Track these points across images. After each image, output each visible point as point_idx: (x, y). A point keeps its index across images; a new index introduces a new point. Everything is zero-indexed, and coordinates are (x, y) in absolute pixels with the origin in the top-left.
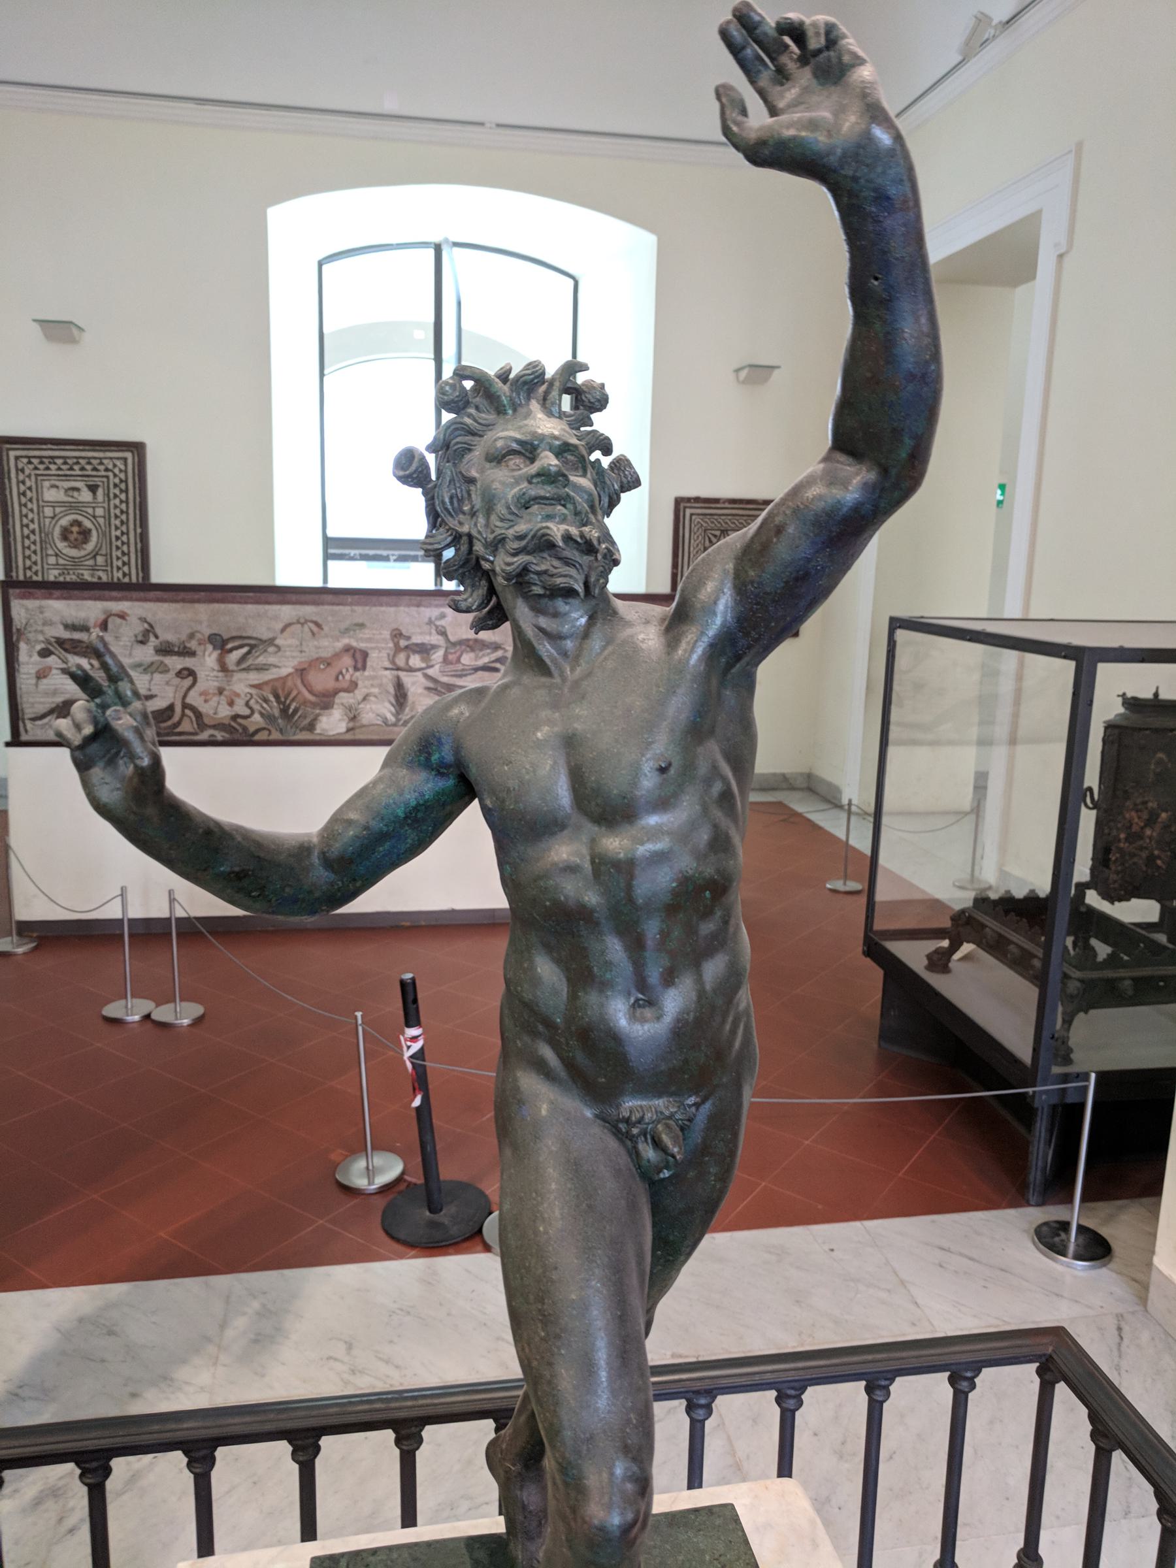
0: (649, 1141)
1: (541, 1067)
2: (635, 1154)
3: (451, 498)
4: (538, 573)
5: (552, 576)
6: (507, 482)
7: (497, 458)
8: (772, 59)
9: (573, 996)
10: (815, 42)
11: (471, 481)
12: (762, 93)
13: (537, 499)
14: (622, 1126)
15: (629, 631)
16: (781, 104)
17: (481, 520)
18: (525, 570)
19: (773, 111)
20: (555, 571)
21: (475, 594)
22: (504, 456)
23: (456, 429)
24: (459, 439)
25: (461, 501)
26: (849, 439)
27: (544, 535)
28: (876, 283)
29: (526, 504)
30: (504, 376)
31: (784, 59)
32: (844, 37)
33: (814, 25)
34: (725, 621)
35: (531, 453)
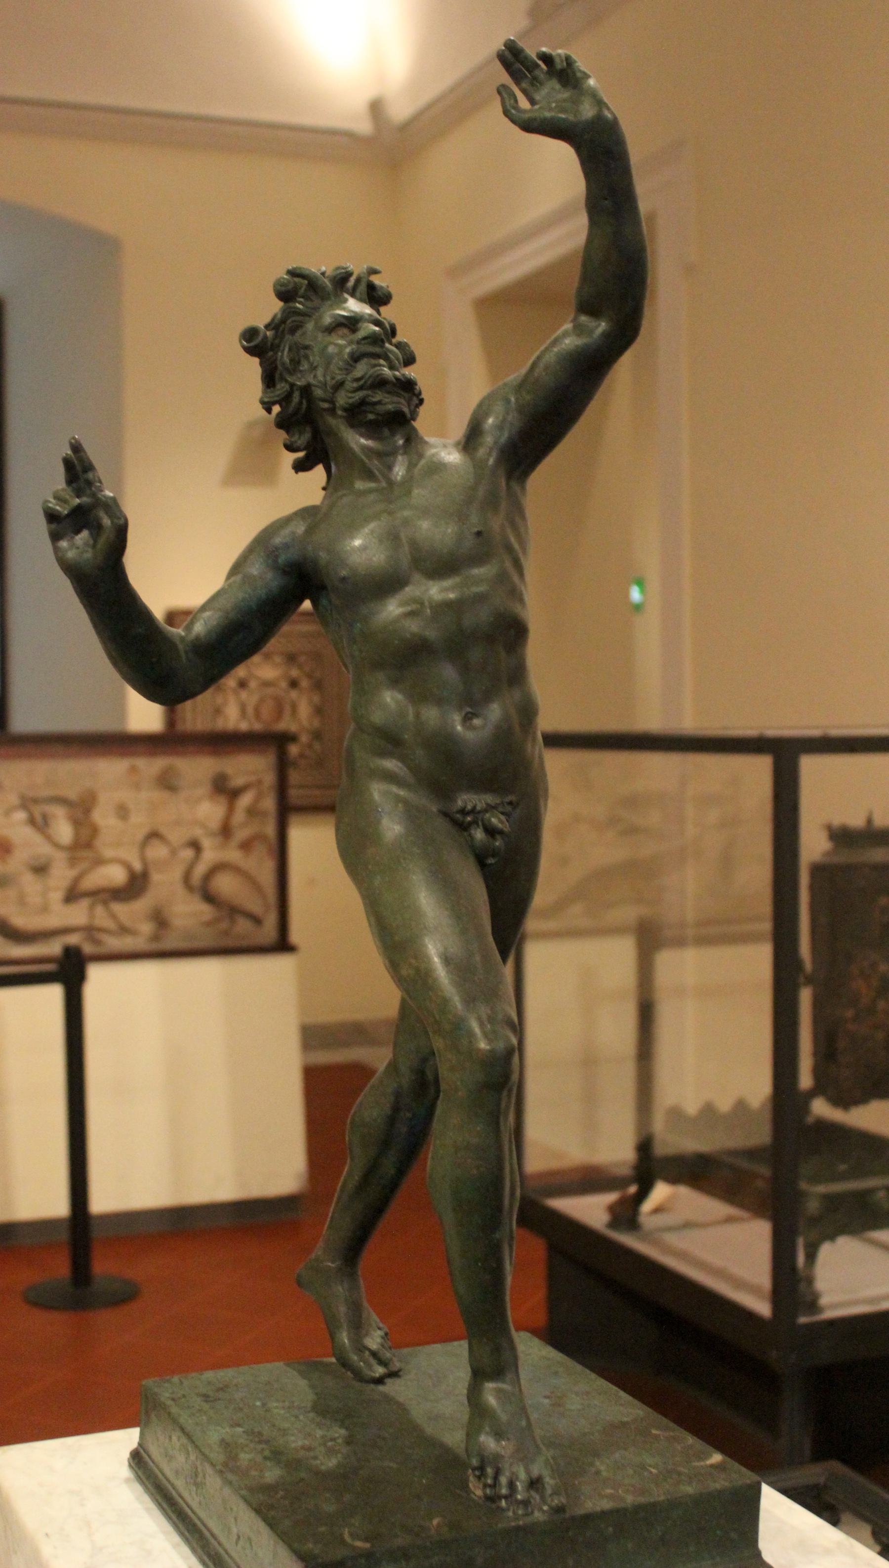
1: (390, 777)
3: (291, 360)
5: (385, 404)
6: (341, 345)
7: (330, 330)
8: (530, 72)
10: (559, 65)
11: (307, 347)
12: (524, 91)
15: (433, 451)
16: (537, 97)
18: (363, 402)
19: (532, 102)
20: (387, 400)
21: (302, 438)
23: (289, 313)
24: (293, 319)
25: (299, 362)
27: (378, 376)
29: (356, 358)
30: (323, 274)
31: (537, 72)
32: (575, 62)
33: (559, 55)
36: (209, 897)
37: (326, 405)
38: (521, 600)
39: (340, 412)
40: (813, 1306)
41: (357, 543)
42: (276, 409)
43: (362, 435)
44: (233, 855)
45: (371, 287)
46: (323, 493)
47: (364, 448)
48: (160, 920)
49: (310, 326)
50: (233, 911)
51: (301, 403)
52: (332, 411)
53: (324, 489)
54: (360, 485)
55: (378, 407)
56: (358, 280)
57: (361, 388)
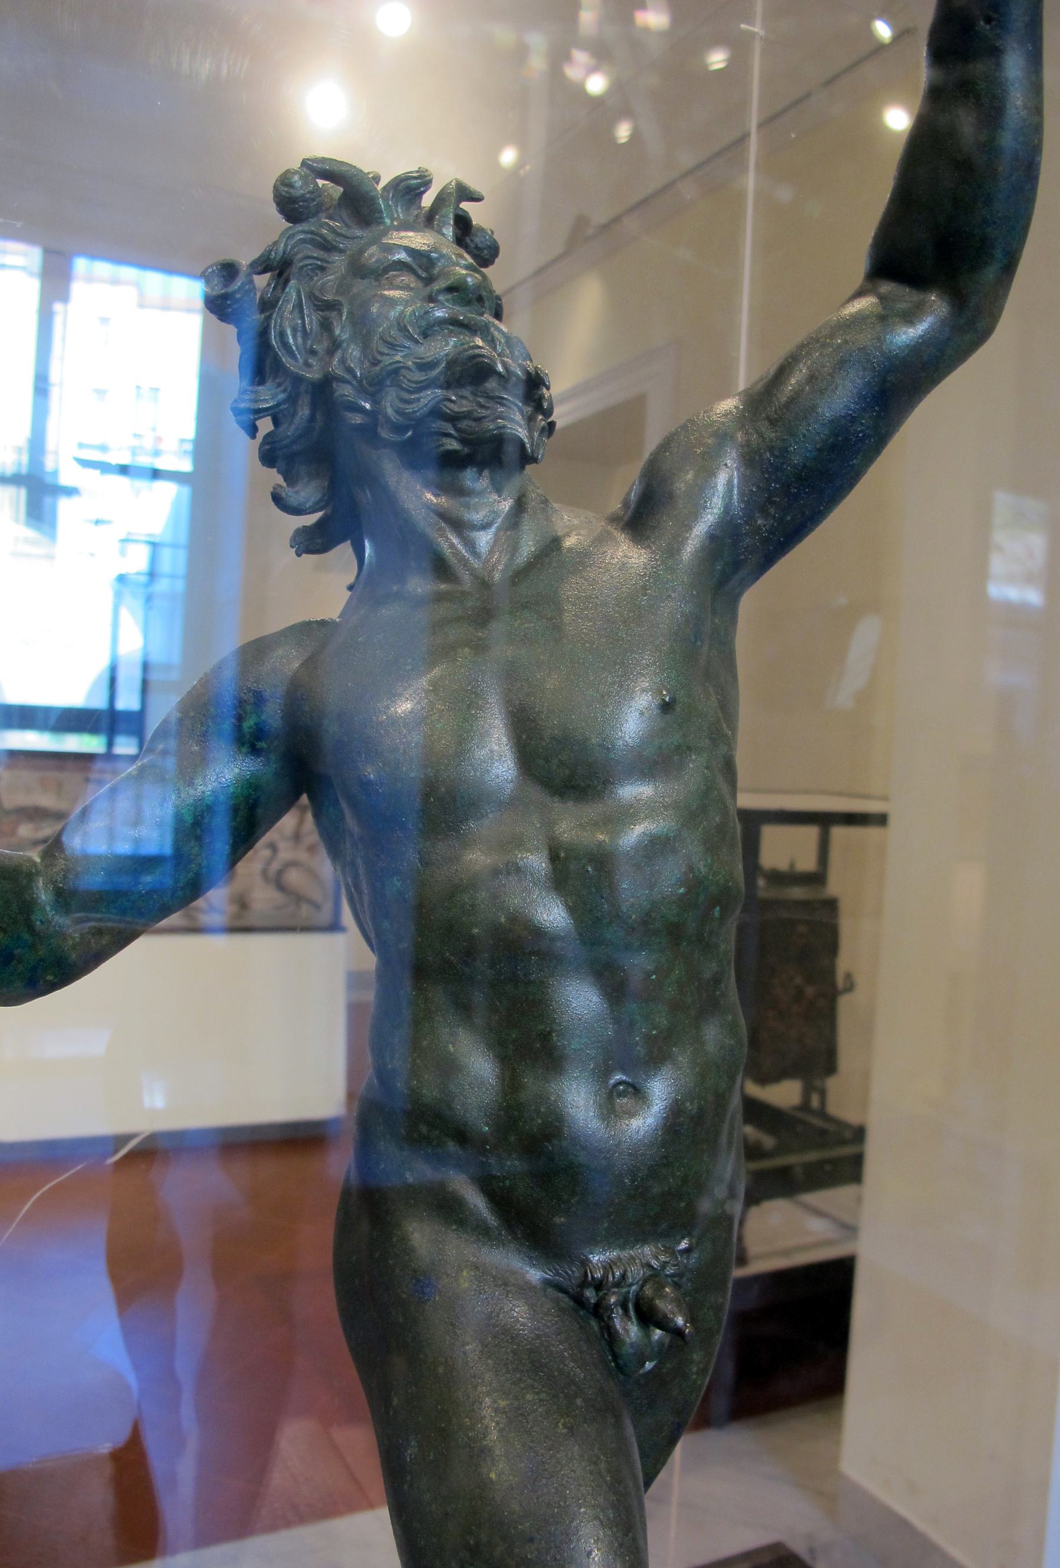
0: (632, 1313)
2: (610, 1336)
3: (294, 330)
4: (454, 419)
9: (511, 1083)
13: (442, 322)
14: (590, 1294)
17: (354, 352)
22: (386, 270)
26: (898, 262)
34: (727, 508)
35: (426, 270)
36: (280, 886)
39: (385, 434)
40: (742, 1260)
41: (404, 707)
42: (265, 425)
43: (427, 485)
44: (302, 855)
45: (463, 223)
46: (350, 593)
47: (428, 506)
48: (242, 903)
50: (298, 898)
51: (312, 418)
53: (351, 588)
56: (441, 200)
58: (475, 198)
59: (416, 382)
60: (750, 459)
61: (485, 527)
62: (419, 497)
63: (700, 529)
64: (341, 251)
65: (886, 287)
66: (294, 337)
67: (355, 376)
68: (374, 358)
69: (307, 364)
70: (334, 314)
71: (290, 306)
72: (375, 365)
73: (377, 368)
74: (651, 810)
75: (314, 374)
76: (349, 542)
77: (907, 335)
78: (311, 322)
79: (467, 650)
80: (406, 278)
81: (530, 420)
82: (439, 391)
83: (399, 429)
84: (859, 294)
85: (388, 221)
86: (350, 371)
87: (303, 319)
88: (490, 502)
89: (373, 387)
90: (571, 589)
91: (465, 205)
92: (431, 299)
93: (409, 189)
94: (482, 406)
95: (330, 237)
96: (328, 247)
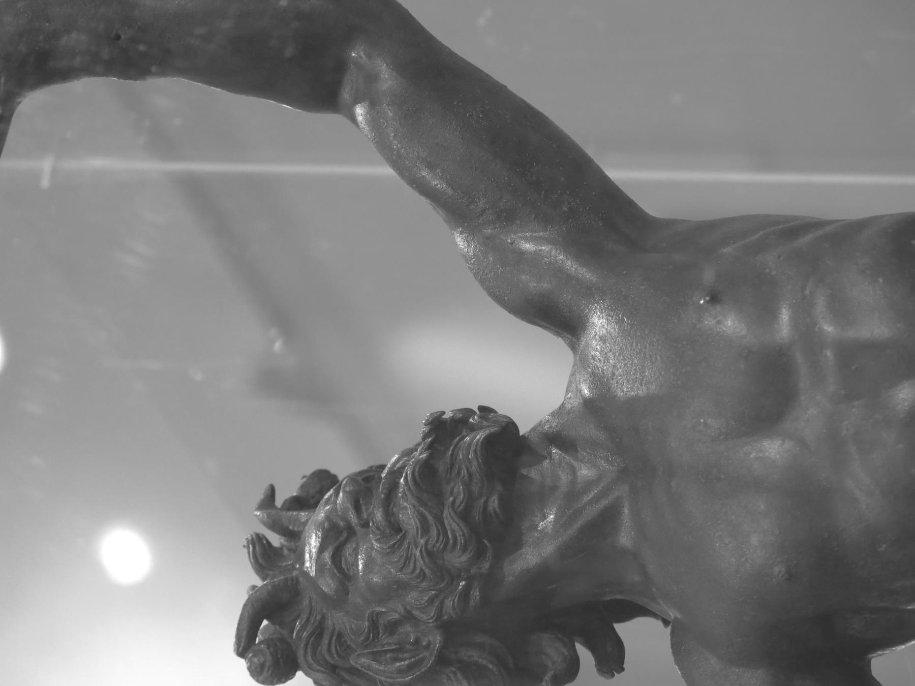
4: (470, 499)
13: (388, 513)
18: (465, 515)
28: (123, 37)
34: (549, 241)
35: (340, 532)
37: (476, 594)
38: (860, 226)
49: (337, 620)
52: (490, 580)
54: (625, 539)
55: (476, 489)
56: (276, 526)
57: (440, 520)
58: (271, 493)
59: (439, 534)
60: (507, 218)
61: (573, 471)
62: (546, 532)
63: (571, 266)
64: (324, 618)
65: (346, 95)
66: (404, 660)
67: (436, 596)
68: (418, 577)
69: (427, 647)
70: (382, 621)
71: (375, 665)
72: (424, 574)
73: (427, 571)
74: (803, 310)
75: (437, 639)
76: (619, 628)
77: (387, 78)
78: (389, 644)
79: (673, 484)
80: (348, 550)
81: (473, 429)
82: (446, 513)
83: (480, 554)
84: (353, 119)
85: (295, 573)
86: (431, 601)
87: (387, 652)
88: (553, 468)
89: (446, 576)
90: (623, 390)
91: (279, 503)
92: (365, 525)
93: (264, 556)
94: (459, 473)
95: (310, 629)
96: (319, 631)
